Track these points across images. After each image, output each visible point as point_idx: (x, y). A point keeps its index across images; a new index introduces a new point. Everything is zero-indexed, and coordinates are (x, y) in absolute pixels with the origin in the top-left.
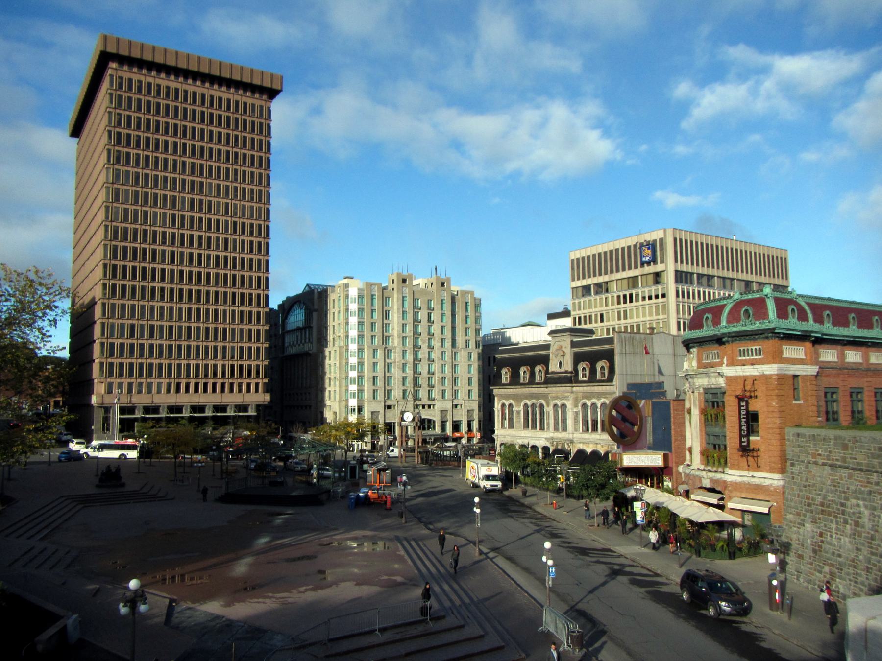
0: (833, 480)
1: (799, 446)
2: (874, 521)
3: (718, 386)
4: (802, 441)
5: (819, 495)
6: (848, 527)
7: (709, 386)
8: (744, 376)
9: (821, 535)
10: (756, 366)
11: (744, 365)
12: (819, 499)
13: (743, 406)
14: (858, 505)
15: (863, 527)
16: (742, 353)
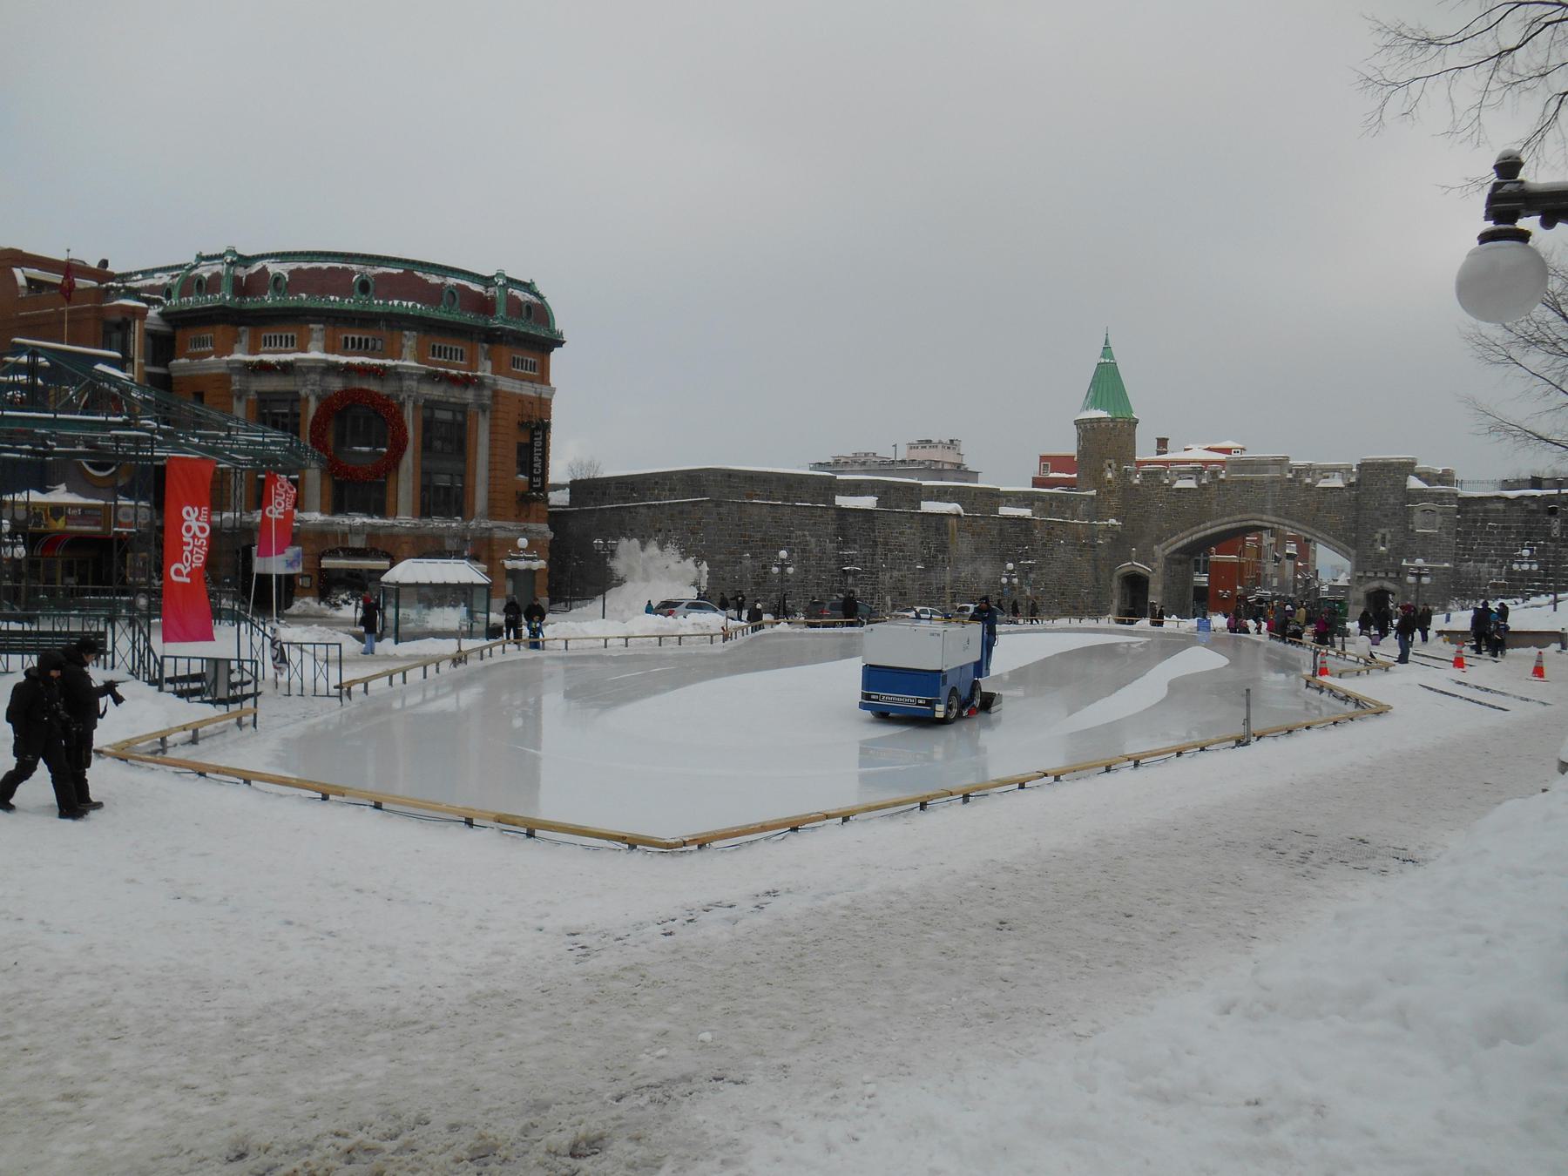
0: (774, 518)
1: (729, 487)
2: (820, 546)
3: (462, 401)
4: (735, 482)
5: (759, 532)
6: (795, 555)
7: (444, 399)
8: (521, 395)
9: (764, 567)
10: (536, 385)
11: (523, 380)
12: (759, 536)
13: (539, 436)
14: (804, 536)
15: (811, 552)
16: (515, 362)
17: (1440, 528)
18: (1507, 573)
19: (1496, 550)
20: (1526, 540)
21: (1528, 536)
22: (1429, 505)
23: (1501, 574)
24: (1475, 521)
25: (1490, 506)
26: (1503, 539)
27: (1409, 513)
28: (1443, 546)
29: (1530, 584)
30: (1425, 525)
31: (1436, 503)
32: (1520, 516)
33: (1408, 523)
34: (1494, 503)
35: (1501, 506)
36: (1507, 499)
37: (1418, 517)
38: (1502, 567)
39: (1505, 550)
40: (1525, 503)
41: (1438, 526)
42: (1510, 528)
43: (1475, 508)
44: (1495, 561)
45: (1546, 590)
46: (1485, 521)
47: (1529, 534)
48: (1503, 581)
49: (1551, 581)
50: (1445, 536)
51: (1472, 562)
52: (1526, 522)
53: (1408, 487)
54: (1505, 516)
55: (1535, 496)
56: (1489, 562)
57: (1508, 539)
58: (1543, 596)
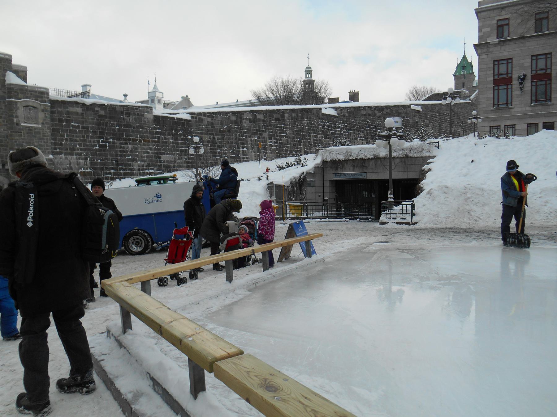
17: (43, 123)
18: (91, 163)
19: (80, 145)
20: (100, 138)
21: (101, 136)
22: (31, 101)
23: (86, 165)
24: (61, 121)
25: (71, 109)
26: (84, 137)
27: (11, 107)
28: (47, 139)
29: (108, 172)
30: (27, 120)
31: (37, 100)
32: (94, 119)
33: (12, 116)
34: (73, 107)
35: (79, 110)
36: (84, 105)
37: (21, 112)
38: (86, 159)
39: (87, 145)
40: (96, 109)
41: (41, 121)
42: (87, 128)
43: (60, 109)
44: (81, 154)
45: (119, 175)
46: (68, 121)
47: (102, 133)
48: (89, 170)
49: (121, 169)
50: (48, 131)
51: (63, 155)
52: (99, 124)
53: (7, 82)
54: (82, 118)
55: (104, 105)
56: (76, 154)
57: (88, 137)
58: (117, 180)
